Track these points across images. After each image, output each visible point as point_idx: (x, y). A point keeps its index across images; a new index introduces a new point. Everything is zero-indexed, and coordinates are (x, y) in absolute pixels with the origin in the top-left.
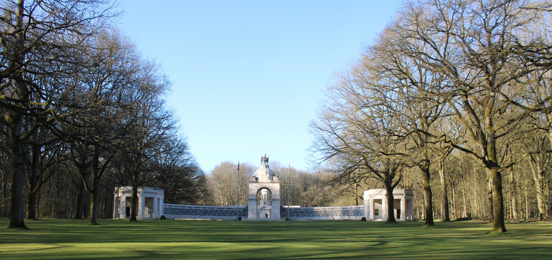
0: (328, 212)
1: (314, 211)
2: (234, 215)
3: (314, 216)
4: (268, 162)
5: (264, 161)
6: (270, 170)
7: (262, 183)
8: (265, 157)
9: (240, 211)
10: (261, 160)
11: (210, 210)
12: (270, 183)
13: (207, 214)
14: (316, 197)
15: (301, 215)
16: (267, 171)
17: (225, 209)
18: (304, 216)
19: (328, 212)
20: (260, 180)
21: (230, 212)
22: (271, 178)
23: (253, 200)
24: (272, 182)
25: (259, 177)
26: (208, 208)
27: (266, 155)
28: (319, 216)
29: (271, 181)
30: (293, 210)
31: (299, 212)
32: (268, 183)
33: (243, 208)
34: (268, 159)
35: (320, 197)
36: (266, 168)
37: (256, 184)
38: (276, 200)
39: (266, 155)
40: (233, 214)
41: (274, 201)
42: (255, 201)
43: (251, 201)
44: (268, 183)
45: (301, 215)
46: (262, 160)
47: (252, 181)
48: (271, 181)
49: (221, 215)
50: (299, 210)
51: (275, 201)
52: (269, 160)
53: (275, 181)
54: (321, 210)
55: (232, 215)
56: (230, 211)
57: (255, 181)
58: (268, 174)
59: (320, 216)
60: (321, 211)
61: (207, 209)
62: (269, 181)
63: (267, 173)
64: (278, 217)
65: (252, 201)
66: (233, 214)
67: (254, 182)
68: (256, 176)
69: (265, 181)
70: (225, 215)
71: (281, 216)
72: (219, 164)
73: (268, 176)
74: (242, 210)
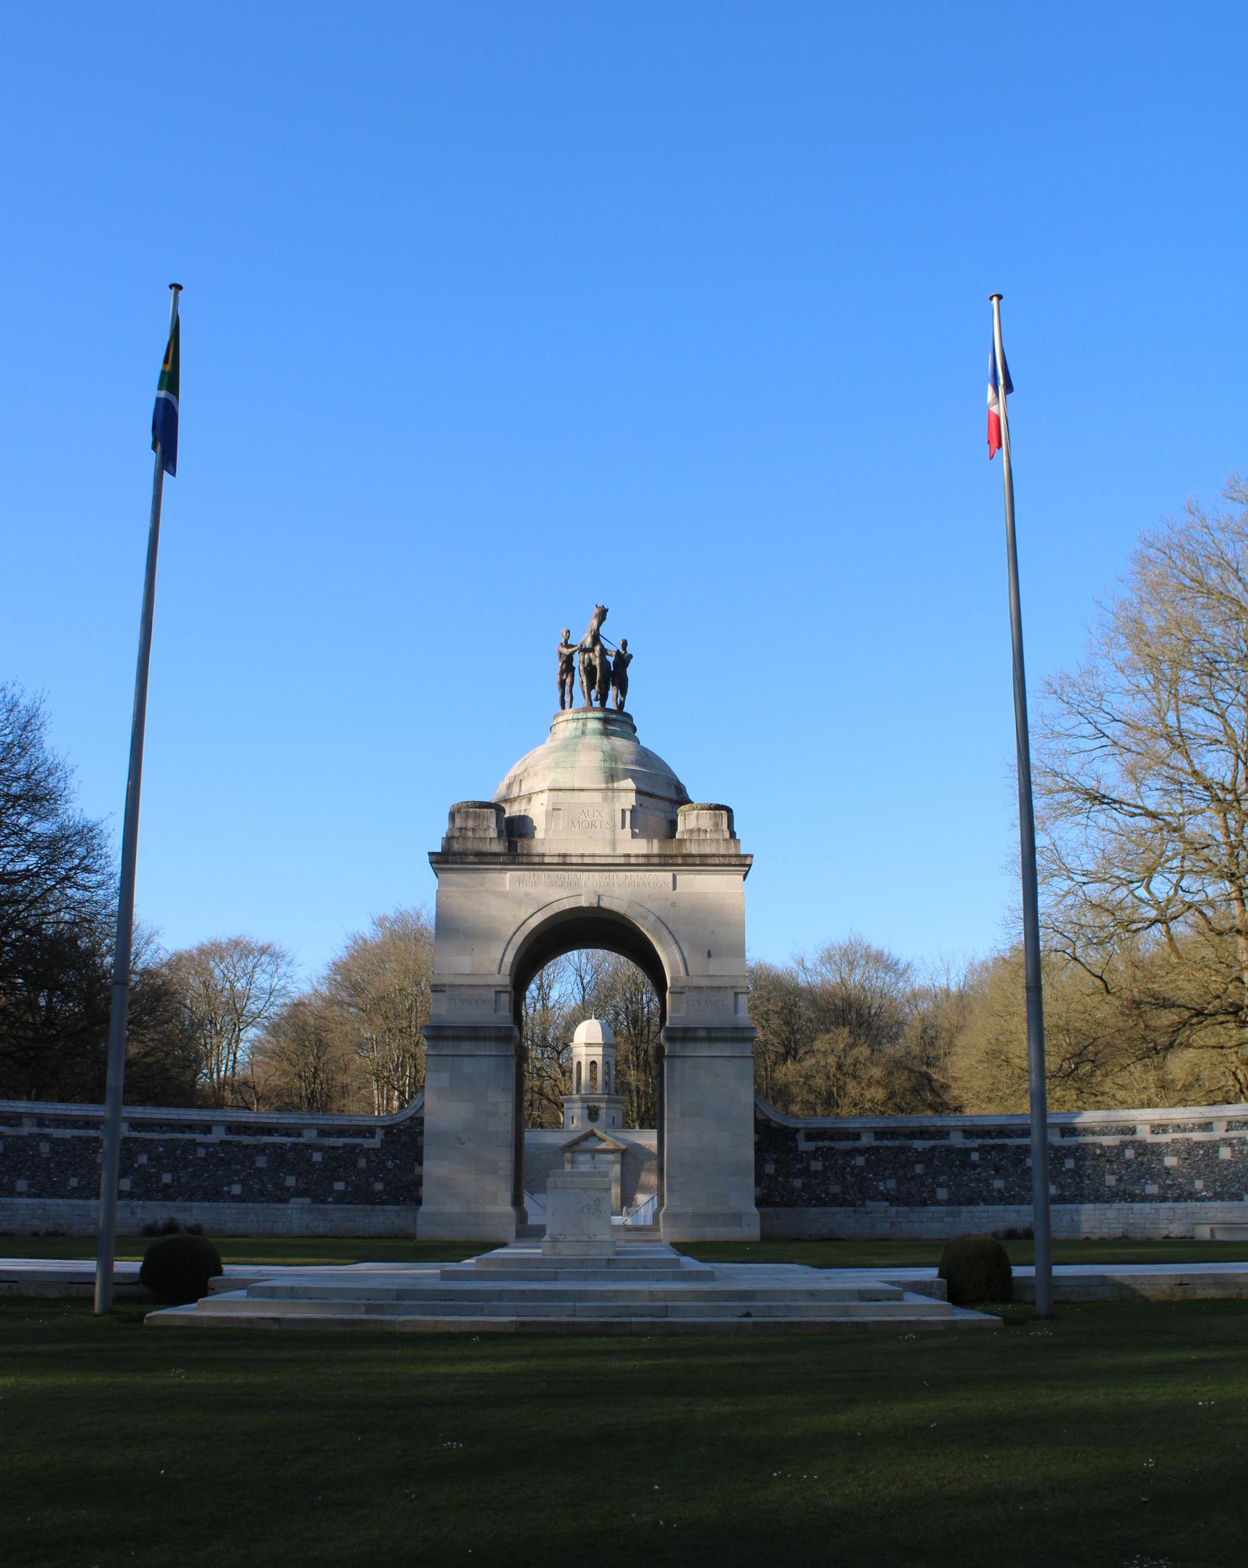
0: (1225, 1153)
1: (1080, 1152)
2: (300, 1193)
3: (1079, 1198)
4: (623, 688)
5: (590, 671)
6: (646, 758)
7: (565, 863)
8: (596, 638)
9: (366, 1152)
10: (558, 665)
11: (55, 1143)
12: (648, 863)
13: (22, 1185)
14: (852, 1088)
15: (942, 1194)
16: (612, 757)
17: (218, 1135)
18: (971, 1201)
19: (1225, 1153)
20: (546, 839)
21: (261, 1162)
22: (656, 819)
23: (474, 1034)
24: (664, 861)
25: (537, 811)
26: (41, 1120)
27: (602, 615)
28: (1133, 1198)
29: (655, 848)
30: (866, 1140)
31: (925, 1157)
32: (627, 864)
33: (388, 1130)
34: (623, 660)
35: (869, 1086)
36: (606, 733)
37: (509, 880)
38: (713, 1035)
39: (602, 615)
40: (291, 1181)
41: (690, 1049)
42: (490, 1049)
43: (448, 1049)
44: (627, 864)
45: (942, 1194)
46: (568, 660)
47: (471, 846)
48: (655, 848)
49: (167, 1194)
50: (919, 1144)
51: (704, 1050)
52: (630, 671)
53: (694, 849)
54: (1144, 1134)
55: (282, 1196)
56: (262, 1149)
57: (497, 847)
58: (629, 783)
59: (1145, 1198)
60: (1144, 1149)
61: (27, 1129)
62: (640, 847)
63: (612, 776)
64: (737, 1218)
65: (466, 1048)
66: (291, 1181)
67: (484, 859)
68: (511, 811)
69: (597, 847)
70: (214, 1195)
71: (759, 1202)
72: (368, 930)
73: (629, 800)
74: (375, 1143)
